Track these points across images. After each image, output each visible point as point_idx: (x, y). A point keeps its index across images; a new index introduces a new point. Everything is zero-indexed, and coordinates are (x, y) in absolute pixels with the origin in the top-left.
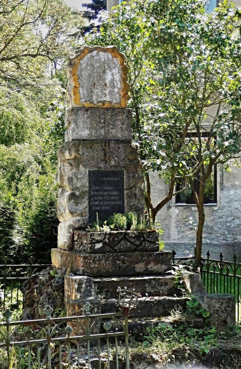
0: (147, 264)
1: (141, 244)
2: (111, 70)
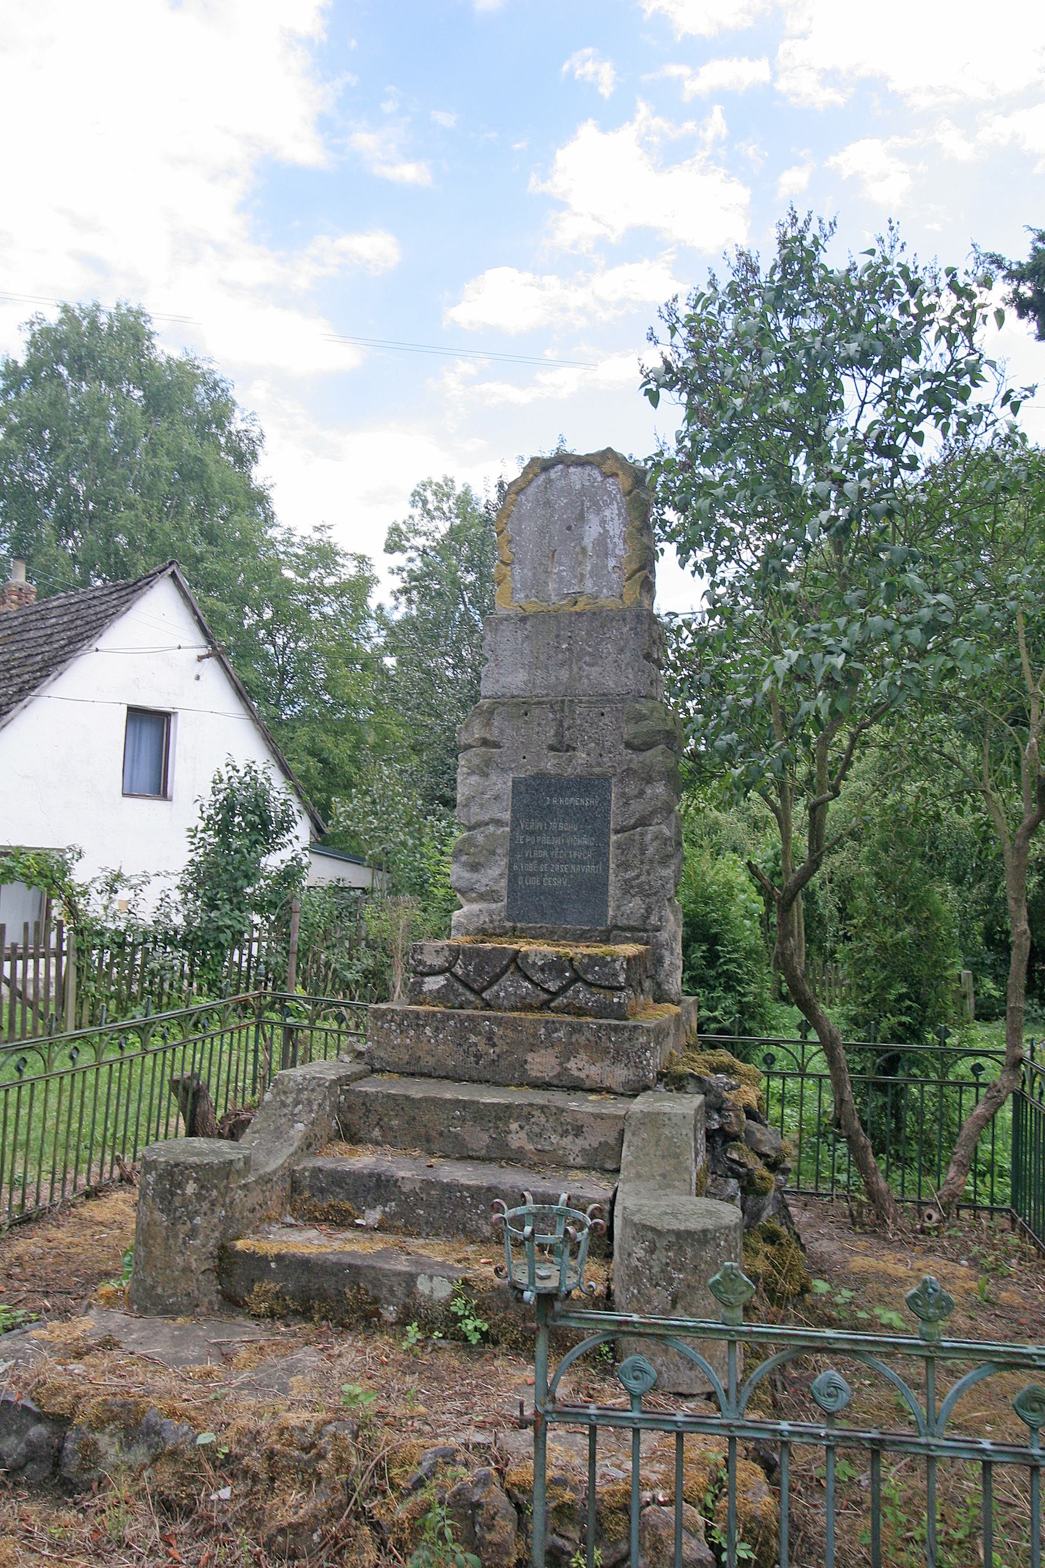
0: (569, 1051)
1: (563, 989)
2: (598, 511)
